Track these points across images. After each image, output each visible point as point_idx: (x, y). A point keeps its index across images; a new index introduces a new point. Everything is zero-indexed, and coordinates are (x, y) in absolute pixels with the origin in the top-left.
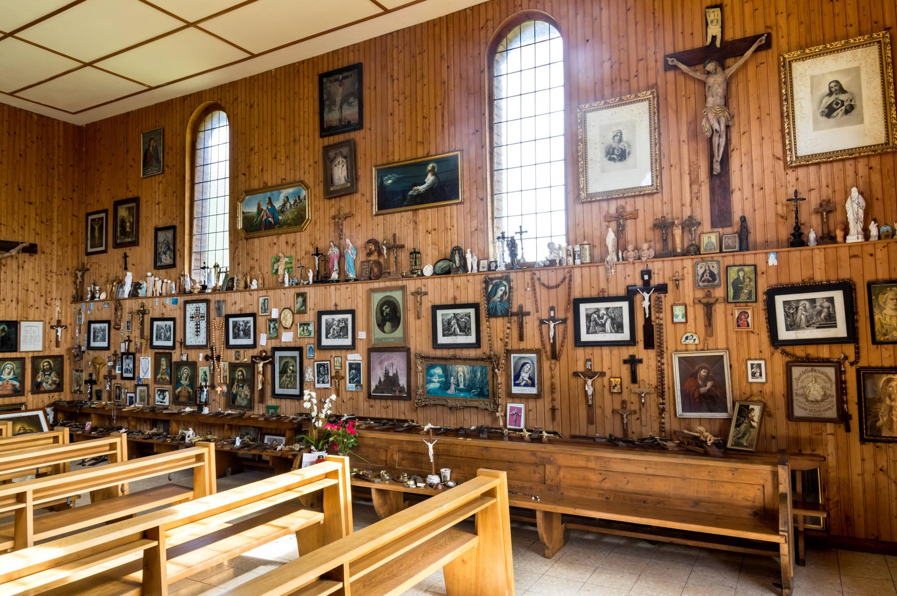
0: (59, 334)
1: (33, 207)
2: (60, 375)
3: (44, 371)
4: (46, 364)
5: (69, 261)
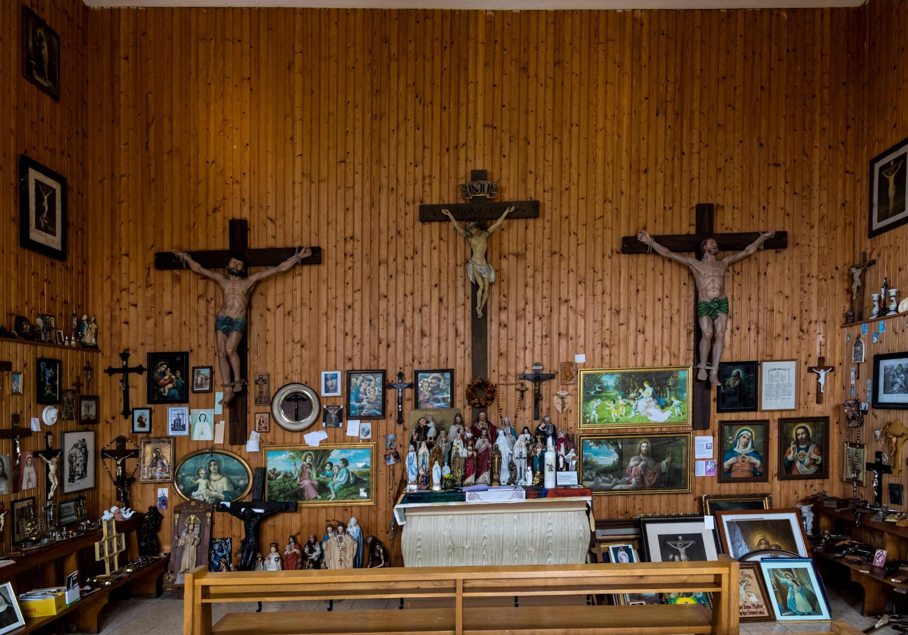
0: (822, 381)
1: (781, 171)
3: (797, 442)
5: (839, 254)
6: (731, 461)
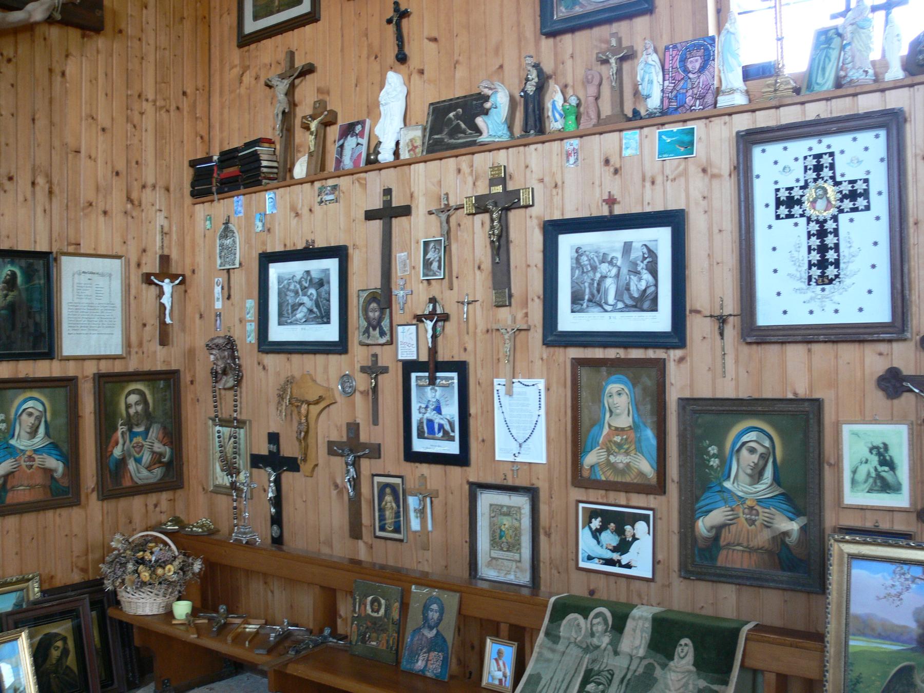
0: (166, 300)
2: (174, 435)
3: (130, 423)
4: (133, 398)
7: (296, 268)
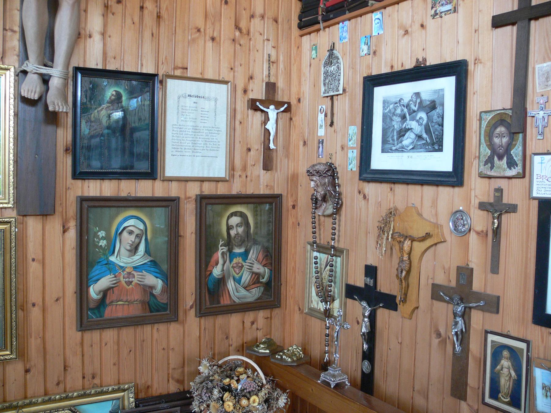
0: (271, 126)
2: (274, 256)
3: (229, 243)
4: (235, 220)
6: (105, 282)
7: (404, 91)
